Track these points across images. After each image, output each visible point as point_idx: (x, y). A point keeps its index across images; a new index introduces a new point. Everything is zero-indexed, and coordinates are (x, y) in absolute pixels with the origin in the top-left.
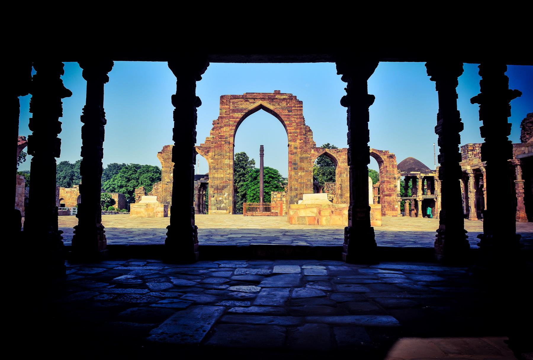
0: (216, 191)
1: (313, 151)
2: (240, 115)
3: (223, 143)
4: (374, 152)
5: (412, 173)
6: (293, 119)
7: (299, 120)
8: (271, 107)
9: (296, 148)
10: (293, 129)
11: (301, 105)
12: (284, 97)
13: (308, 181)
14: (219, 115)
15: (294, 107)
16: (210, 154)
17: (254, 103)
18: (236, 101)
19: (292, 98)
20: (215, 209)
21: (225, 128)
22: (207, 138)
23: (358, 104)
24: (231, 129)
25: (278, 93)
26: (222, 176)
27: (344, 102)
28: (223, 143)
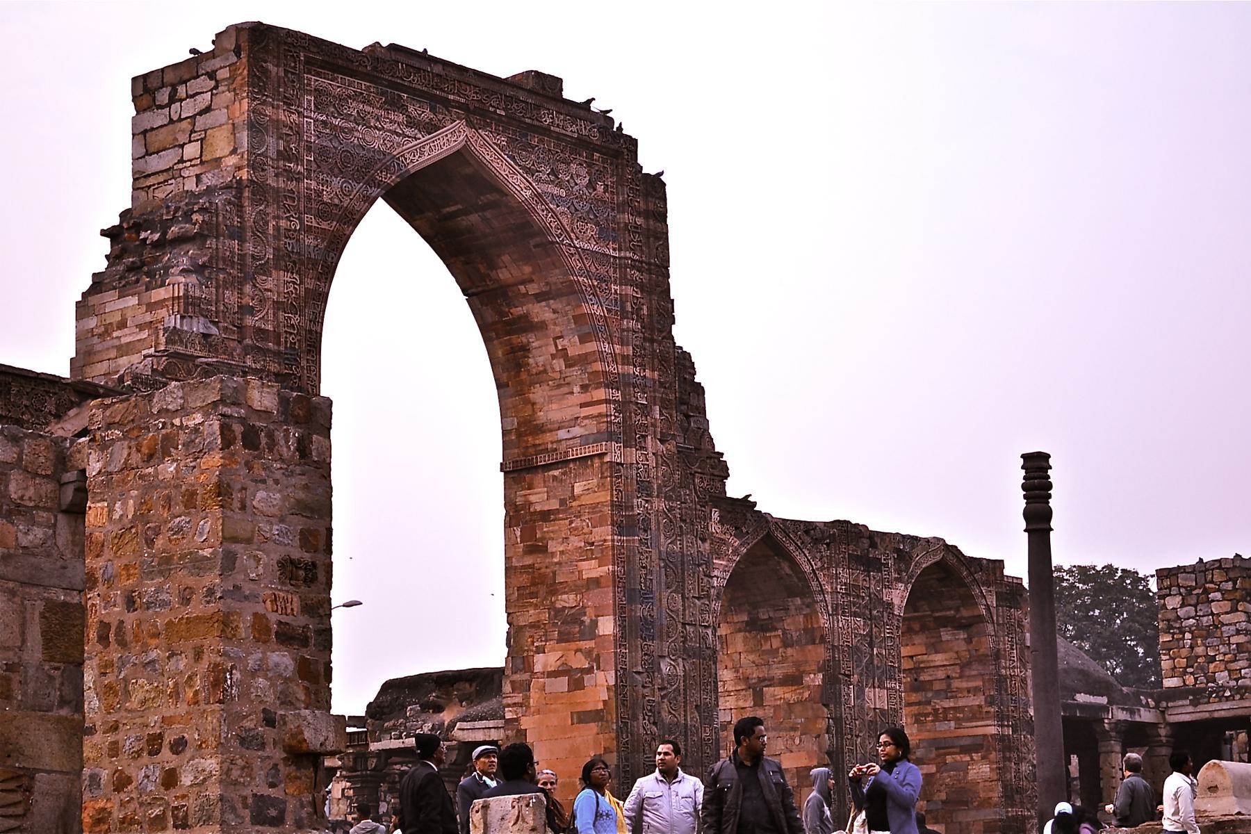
4: (951, 559)
5: (1081, 698)
10: (625, 360)
17: (431, 128)
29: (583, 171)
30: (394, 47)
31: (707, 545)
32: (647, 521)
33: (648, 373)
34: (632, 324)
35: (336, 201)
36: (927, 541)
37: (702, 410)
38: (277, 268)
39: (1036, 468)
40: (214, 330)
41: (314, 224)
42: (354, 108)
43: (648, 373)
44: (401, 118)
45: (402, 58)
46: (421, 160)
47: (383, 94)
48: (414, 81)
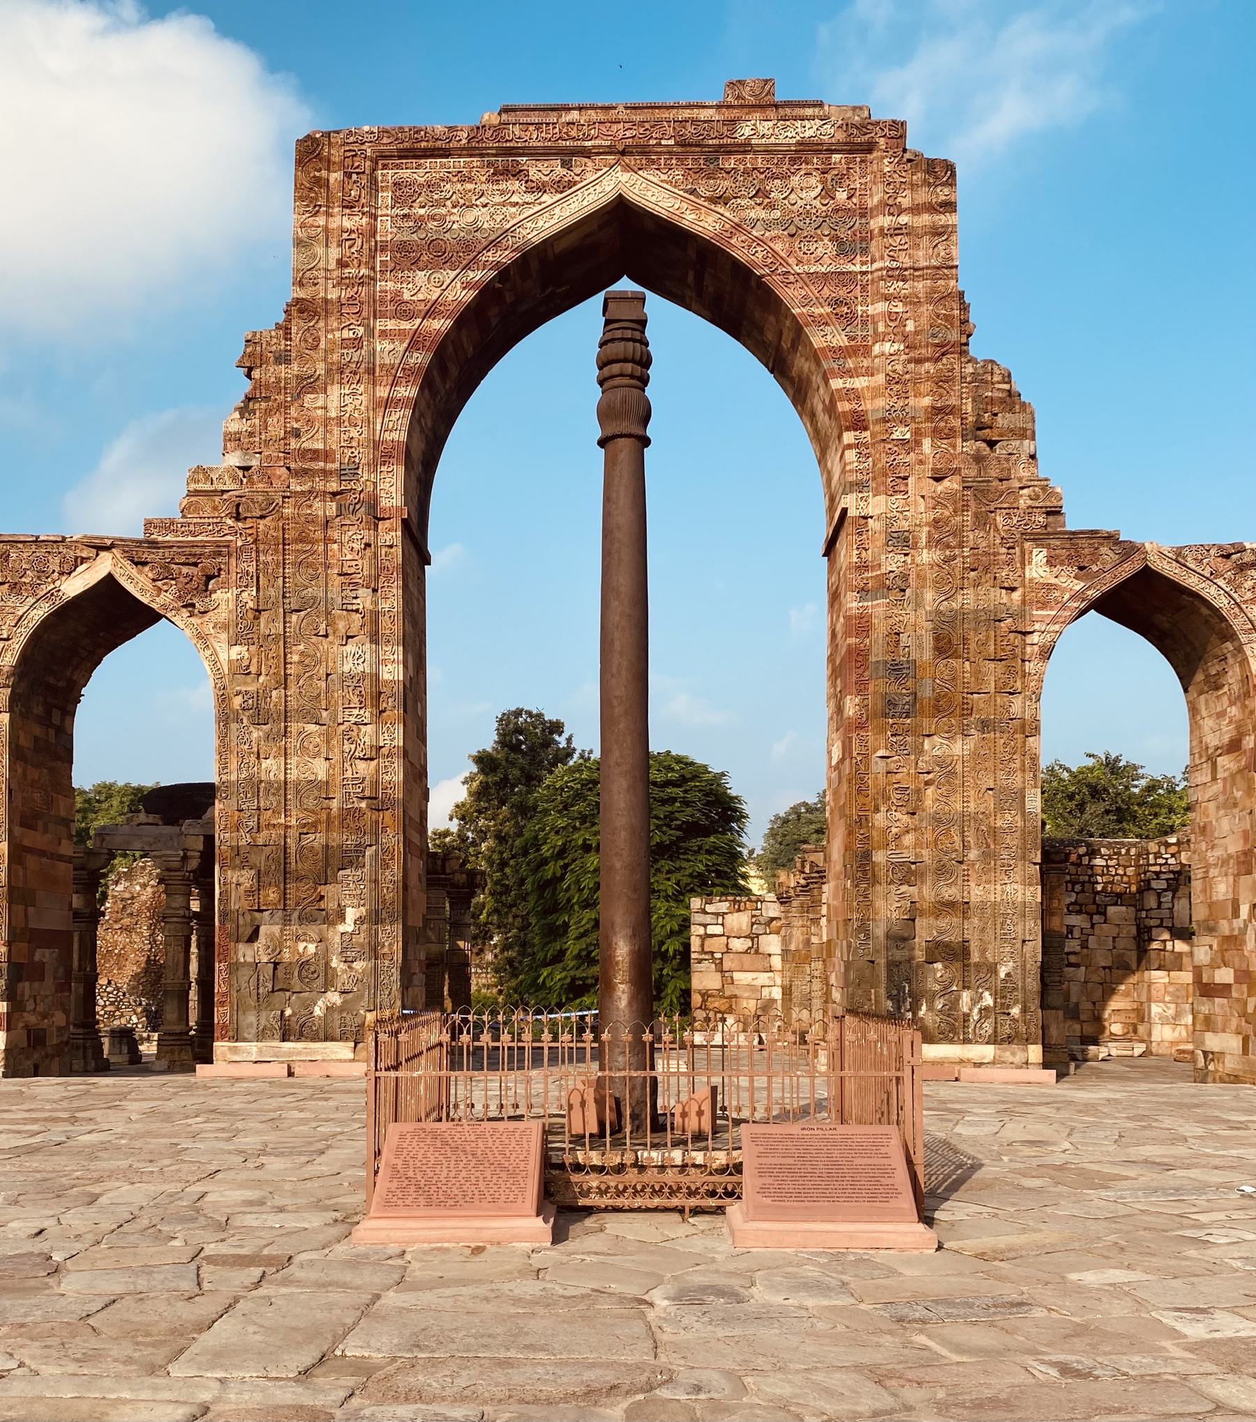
0: (272, 895)
1: (1038, 567)
2: (455, 288)
6: (880, 307)
8: (704, 222)
9: (902, 541)
11: (943, 194)
12: (809, 130)
13: (1000, 808)
16: (224, 599)
17: (562, 186)
20: (261, 1036)
21: (335, 391)
22: (201, 472)
24: (388, 403)
26: (320, 769)
28: (332, 508)
30: (506, 110)
31: (1016, 595)
32: (905, 577)
34: (887, 347)
35: (420, 296)
37: (1026, 433)
38: (332, 384)
41: (391, 324)
44: (515, 185)
46: (547, 225)
47: (490, 164)
48: (534, 138)
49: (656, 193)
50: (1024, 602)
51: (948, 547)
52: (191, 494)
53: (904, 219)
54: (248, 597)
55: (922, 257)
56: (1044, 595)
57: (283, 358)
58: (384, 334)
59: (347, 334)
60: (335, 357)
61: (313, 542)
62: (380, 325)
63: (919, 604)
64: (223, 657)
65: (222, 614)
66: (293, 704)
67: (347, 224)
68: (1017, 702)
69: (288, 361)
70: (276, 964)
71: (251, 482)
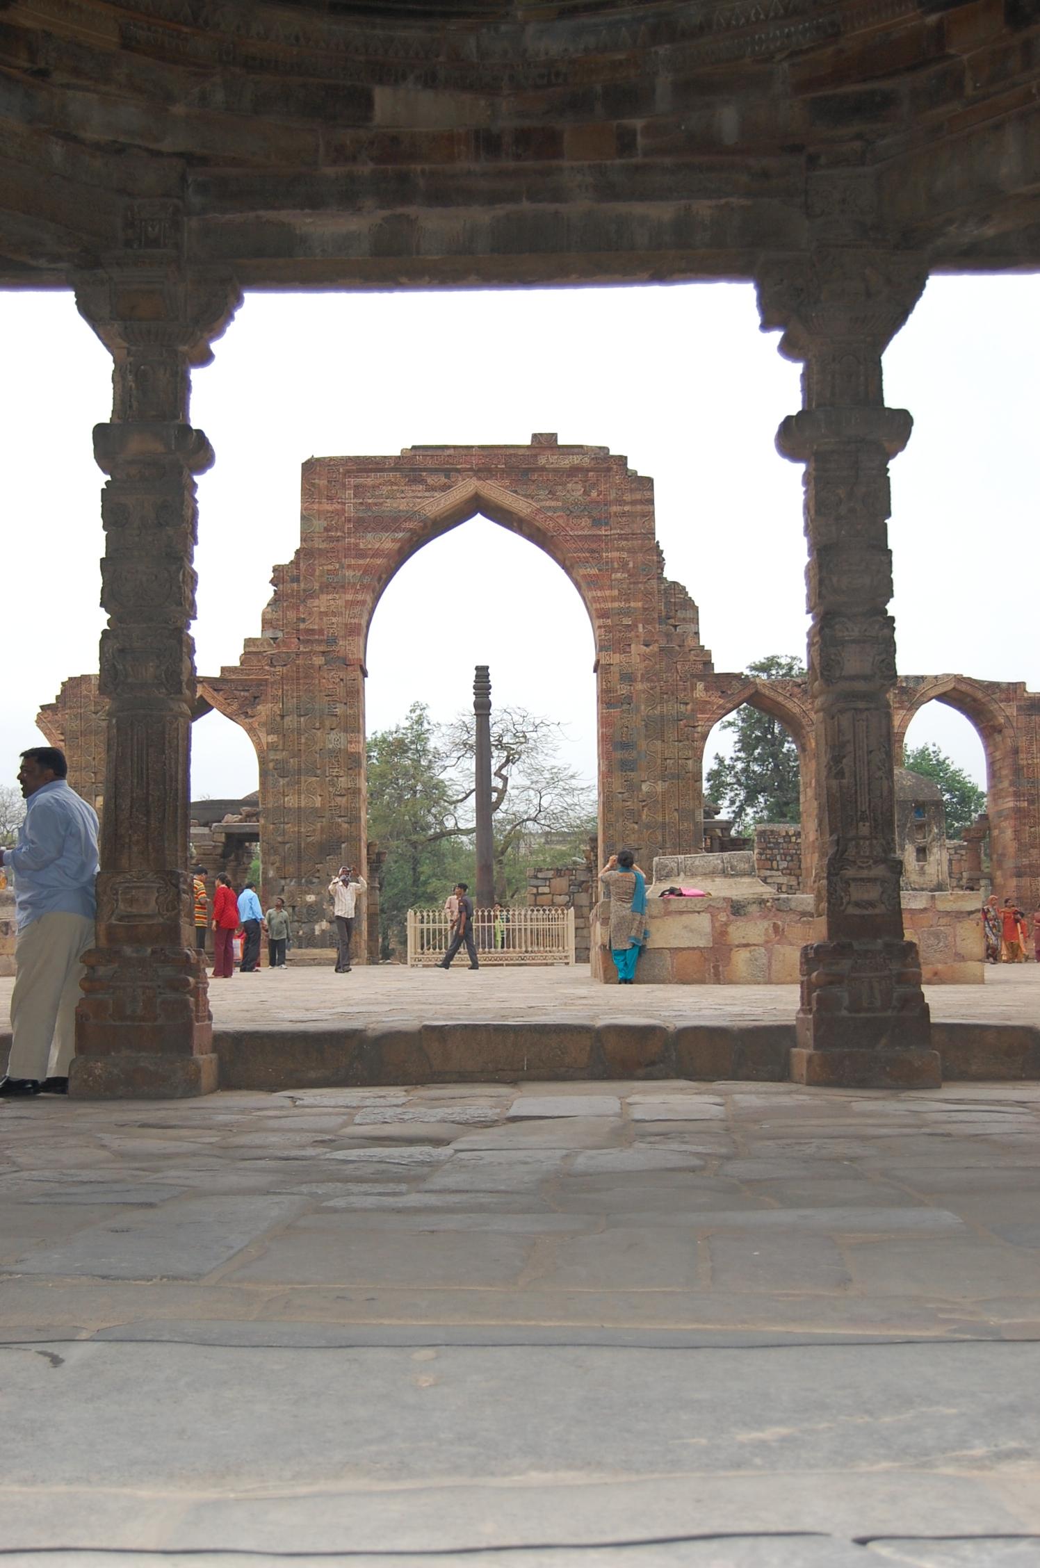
0: (291, 869)
2: (388, 542)
3: (318, 661)
4: (963, 687)
7: (640, 557)
9: (628, 678)
10: (613, 599)
12: (576, 460)
14: (298, 546)
15: (621, 502)
16: (264, 710)
17: (445, 488)
18: (370, 480)
19: (605, 467)
21: (324, 597)
22: (249, 642)
23: (846, 448)
25: (545, 442)
27: (792, 437)
29: (579, 486)
30: (414, 448)
31: (689, 707)
33: (632, 604)
36: (936, 677)
37: (695, 620)
38: (322, 593)
39: (482, 674)
40: (280, 635)
42: (385, 490)
43: (632, 604)
45: (421, 452)
48: (430, 464)
49: (494, 491)
50: (693, 710)
51: (652, 681)
52: (245, 653)
53: (627, 508)
54: (277, 708)
55: (637, 527)
56: (703, 706)
57: (296, 579)
58: (349, 566)
59: (330, 567)
60: (324, 579)
61: (313, 678)
62: (346, 561)
63: (638, 711)
64: (264, 741)
65: (264, 719)
66: (303, 766)
67: (329, 508)
68: (690, 762)
69: (298, 581)
70: (294, 907)
71: (278, 646)
